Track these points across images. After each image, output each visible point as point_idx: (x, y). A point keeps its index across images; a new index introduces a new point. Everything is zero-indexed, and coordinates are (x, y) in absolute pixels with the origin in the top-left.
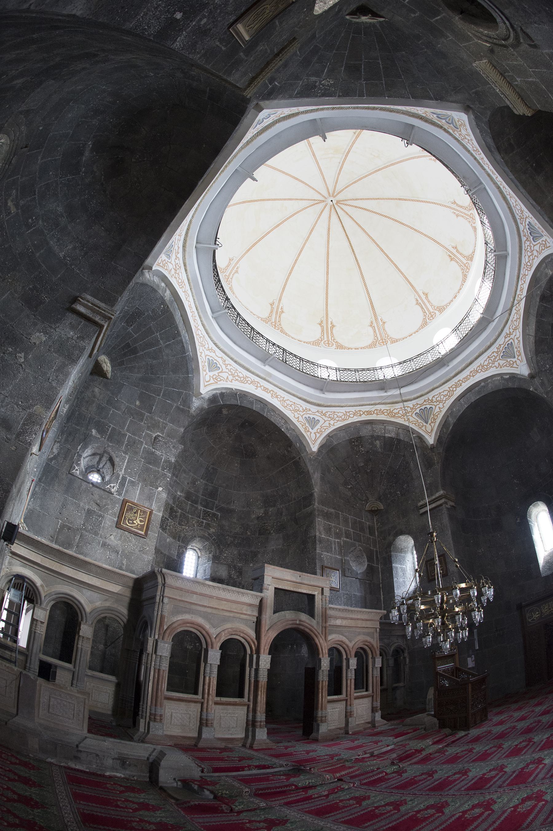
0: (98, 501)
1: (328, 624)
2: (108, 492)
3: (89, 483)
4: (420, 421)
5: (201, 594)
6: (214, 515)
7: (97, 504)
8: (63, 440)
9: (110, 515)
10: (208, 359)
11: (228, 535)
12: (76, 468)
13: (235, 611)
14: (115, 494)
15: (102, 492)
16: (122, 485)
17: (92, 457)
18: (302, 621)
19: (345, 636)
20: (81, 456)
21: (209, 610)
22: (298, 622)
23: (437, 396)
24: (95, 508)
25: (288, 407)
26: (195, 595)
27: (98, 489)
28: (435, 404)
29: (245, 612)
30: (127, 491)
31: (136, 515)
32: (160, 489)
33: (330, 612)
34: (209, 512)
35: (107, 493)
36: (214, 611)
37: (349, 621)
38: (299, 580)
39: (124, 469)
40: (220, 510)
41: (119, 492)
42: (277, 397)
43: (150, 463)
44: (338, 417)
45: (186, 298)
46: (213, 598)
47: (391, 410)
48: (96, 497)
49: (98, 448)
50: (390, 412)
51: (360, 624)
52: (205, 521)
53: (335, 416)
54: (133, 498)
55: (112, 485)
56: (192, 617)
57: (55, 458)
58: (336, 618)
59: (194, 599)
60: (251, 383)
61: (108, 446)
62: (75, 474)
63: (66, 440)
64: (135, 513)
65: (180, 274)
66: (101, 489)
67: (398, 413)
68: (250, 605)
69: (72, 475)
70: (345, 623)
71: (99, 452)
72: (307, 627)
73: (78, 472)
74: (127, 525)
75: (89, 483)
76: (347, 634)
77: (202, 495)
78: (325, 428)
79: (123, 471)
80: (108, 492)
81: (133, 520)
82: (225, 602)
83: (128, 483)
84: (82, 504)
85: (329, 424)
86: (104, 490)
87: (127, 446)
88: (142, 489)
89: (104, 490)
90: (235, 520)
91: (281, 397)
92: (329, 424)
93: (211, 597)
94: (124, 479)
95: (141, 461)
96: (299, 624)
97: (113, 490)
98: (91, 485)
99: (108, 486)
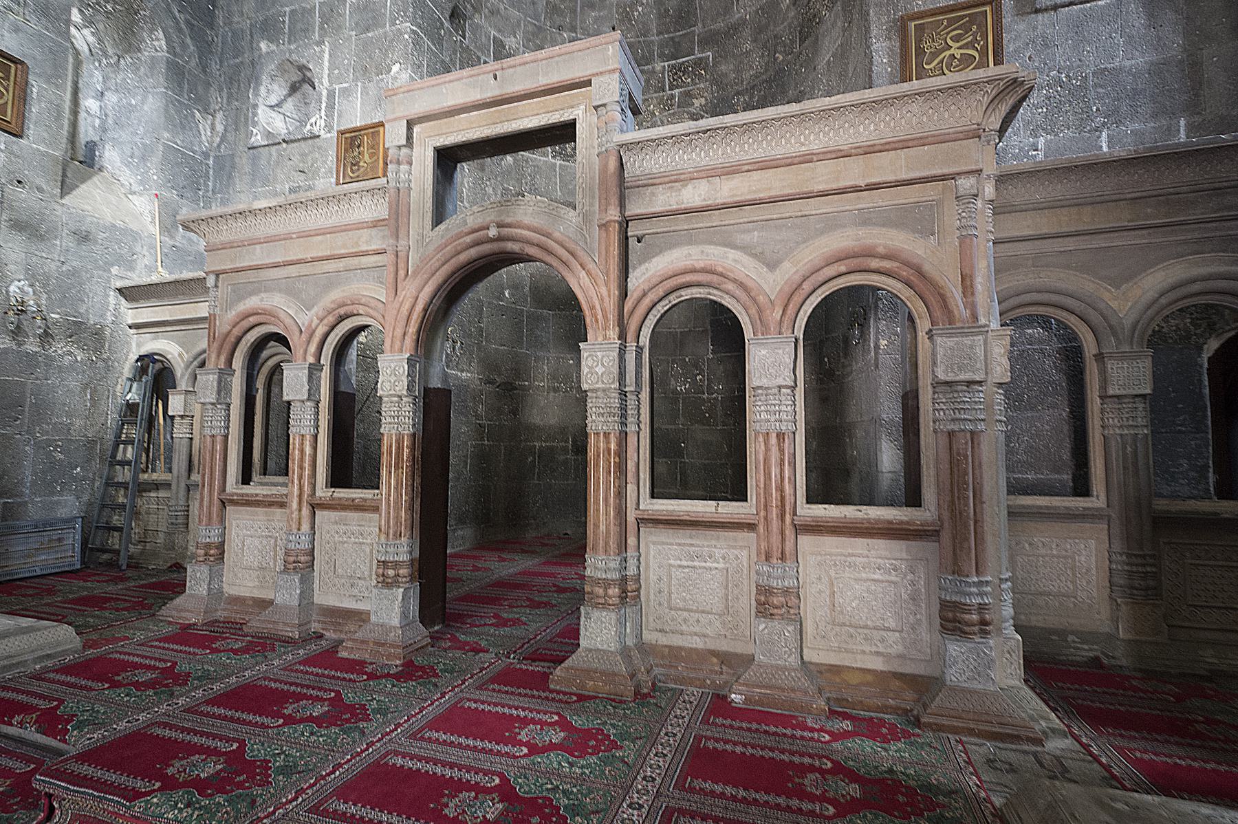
0: (301, 165)
1: (633, 209)
2: (311, 138)
3: (279, 143)
5: (269, 240)
6: (698, 63)
7: (300, 171)
8: (225, 101)
9: (323, 178)
11: (738, 93)
12: (255, 131)
13: (343, 251)
14: (322, 133)
15: (302, 144)
16: (331, 107)
17: (298, 95)
18: (509, 226)
19: (743, 248)
20: (255, 106)
21: (292, 271)
22: (493, 232)
24: (300, 180)
26: (258, 247)
27: (296, 144)
29: (364, 248)
30: (340, 116)
31: (362, 148)
32: (395, 68)
33: (637, 166)
34: (683, 63)
35: (310, 142)
36: (304, 269)
37: (756, 175)
38: (492, 90)
39: (326, 76)
40: (705, 42)
41: (329, 127)
43: (367, 30)
46: (292, 238)
48: (296, 159)
49: (282, 69)
51: (822, 176)
52: (677, 91)
54: (354, 119)
55: (313, 120)
56: (262, 300)
57: (223, 139)
58: (678, 179)
59: (258, 256)
61: (291, 52)
62: (255, 145)
63: (230, 96)
64: (359, 147)
66: (299, 140)
68: (375, 224)
69: (254, 148)
70: (727, 190)
71: (295, 78)
72: (529, 242)
73: (259, 137)
74: (352, 178)
75: (279, 143)
76: (746, 238)
77: (659, 33)
79: (326, 81)
80: (311, 138)
81: (356, 164)
82: (320, 238)
83: (339, 98)
84: (278, 187)
86: (305, 139)
87: (322, 28)
88: (365, 91)
89: (305, 139)
90: (748, 46)
93: (287, 237)
94: (331, 94)
95: (351, 36)
96: (500, 239)
97: (316, 130)
98: (284, 145)
99: (308, 127)
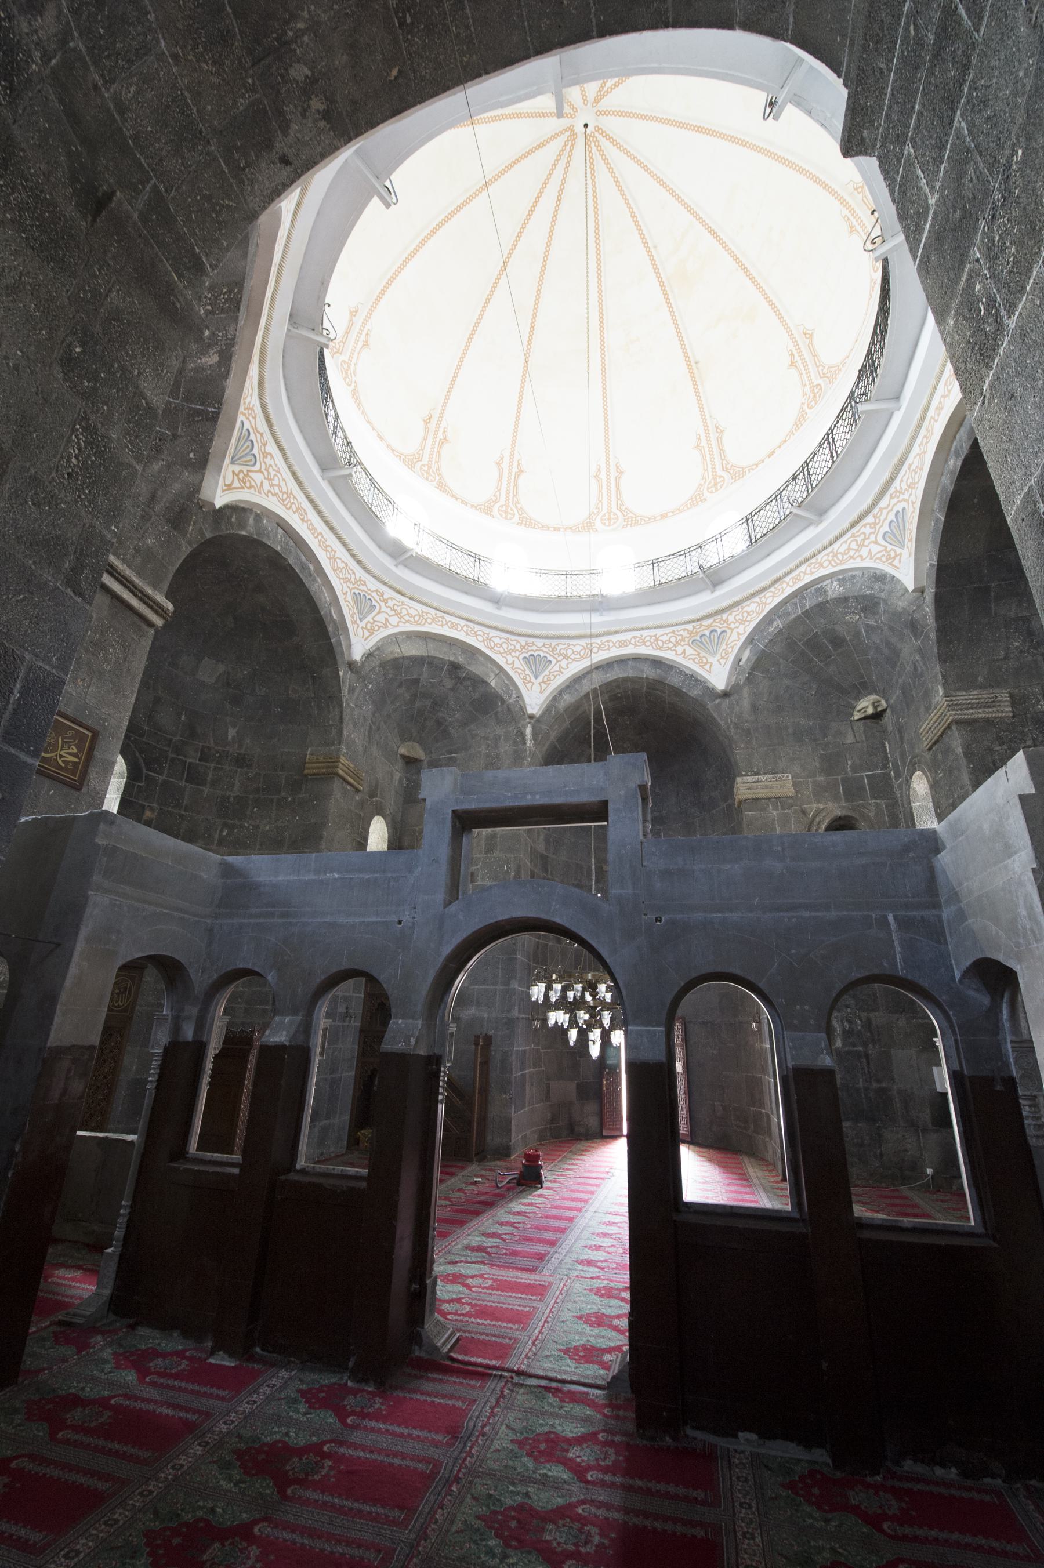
4: (890, 547)
10: (525, 658)
23: (907, 476)
25: (665, 646)
28: (906, 496)
42: (644, 643)
44: (748, 613)
45: (442, 625)
47: (835, 551)
50: (833, 556)
53: (745, 614)
60: (599, 649)
65: (411, 611)
67: (849, 549)
78: (732, 644)
85: (739, 634)
91: (651, 637)
92: (739, 634)
